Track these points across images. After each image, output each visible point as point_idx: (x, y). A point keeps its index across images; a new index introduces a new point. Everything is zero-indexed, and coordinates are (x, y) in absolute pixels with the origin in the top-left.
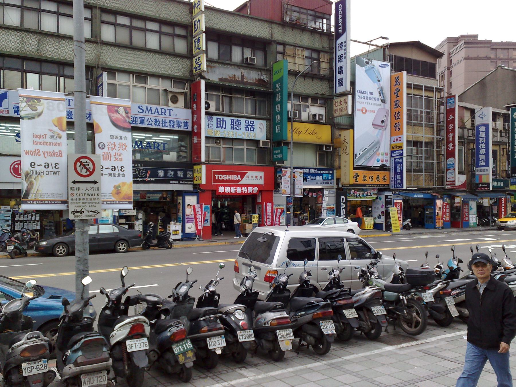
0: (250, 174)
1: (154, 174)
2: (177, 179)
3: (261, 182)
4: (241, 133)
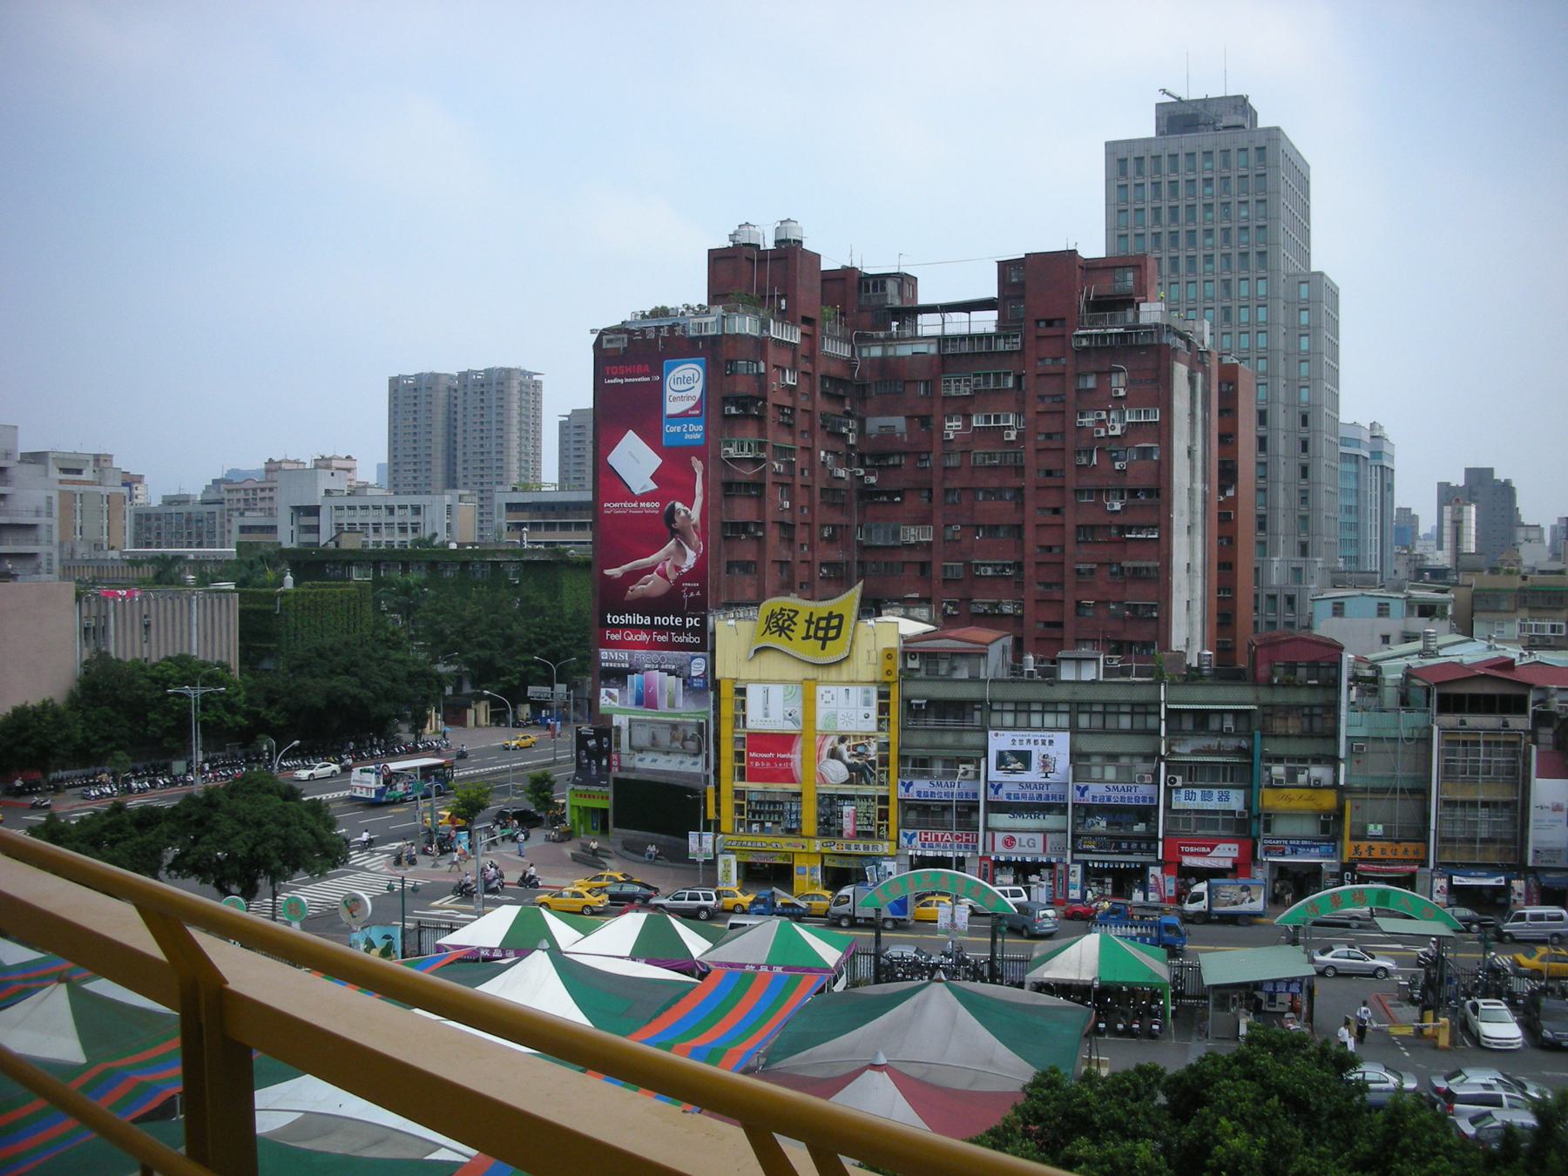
0: (1221, 846)
1: (1118, 846)
2: (1140, 850)
3: (1236, 854)
4: (1214, 804)
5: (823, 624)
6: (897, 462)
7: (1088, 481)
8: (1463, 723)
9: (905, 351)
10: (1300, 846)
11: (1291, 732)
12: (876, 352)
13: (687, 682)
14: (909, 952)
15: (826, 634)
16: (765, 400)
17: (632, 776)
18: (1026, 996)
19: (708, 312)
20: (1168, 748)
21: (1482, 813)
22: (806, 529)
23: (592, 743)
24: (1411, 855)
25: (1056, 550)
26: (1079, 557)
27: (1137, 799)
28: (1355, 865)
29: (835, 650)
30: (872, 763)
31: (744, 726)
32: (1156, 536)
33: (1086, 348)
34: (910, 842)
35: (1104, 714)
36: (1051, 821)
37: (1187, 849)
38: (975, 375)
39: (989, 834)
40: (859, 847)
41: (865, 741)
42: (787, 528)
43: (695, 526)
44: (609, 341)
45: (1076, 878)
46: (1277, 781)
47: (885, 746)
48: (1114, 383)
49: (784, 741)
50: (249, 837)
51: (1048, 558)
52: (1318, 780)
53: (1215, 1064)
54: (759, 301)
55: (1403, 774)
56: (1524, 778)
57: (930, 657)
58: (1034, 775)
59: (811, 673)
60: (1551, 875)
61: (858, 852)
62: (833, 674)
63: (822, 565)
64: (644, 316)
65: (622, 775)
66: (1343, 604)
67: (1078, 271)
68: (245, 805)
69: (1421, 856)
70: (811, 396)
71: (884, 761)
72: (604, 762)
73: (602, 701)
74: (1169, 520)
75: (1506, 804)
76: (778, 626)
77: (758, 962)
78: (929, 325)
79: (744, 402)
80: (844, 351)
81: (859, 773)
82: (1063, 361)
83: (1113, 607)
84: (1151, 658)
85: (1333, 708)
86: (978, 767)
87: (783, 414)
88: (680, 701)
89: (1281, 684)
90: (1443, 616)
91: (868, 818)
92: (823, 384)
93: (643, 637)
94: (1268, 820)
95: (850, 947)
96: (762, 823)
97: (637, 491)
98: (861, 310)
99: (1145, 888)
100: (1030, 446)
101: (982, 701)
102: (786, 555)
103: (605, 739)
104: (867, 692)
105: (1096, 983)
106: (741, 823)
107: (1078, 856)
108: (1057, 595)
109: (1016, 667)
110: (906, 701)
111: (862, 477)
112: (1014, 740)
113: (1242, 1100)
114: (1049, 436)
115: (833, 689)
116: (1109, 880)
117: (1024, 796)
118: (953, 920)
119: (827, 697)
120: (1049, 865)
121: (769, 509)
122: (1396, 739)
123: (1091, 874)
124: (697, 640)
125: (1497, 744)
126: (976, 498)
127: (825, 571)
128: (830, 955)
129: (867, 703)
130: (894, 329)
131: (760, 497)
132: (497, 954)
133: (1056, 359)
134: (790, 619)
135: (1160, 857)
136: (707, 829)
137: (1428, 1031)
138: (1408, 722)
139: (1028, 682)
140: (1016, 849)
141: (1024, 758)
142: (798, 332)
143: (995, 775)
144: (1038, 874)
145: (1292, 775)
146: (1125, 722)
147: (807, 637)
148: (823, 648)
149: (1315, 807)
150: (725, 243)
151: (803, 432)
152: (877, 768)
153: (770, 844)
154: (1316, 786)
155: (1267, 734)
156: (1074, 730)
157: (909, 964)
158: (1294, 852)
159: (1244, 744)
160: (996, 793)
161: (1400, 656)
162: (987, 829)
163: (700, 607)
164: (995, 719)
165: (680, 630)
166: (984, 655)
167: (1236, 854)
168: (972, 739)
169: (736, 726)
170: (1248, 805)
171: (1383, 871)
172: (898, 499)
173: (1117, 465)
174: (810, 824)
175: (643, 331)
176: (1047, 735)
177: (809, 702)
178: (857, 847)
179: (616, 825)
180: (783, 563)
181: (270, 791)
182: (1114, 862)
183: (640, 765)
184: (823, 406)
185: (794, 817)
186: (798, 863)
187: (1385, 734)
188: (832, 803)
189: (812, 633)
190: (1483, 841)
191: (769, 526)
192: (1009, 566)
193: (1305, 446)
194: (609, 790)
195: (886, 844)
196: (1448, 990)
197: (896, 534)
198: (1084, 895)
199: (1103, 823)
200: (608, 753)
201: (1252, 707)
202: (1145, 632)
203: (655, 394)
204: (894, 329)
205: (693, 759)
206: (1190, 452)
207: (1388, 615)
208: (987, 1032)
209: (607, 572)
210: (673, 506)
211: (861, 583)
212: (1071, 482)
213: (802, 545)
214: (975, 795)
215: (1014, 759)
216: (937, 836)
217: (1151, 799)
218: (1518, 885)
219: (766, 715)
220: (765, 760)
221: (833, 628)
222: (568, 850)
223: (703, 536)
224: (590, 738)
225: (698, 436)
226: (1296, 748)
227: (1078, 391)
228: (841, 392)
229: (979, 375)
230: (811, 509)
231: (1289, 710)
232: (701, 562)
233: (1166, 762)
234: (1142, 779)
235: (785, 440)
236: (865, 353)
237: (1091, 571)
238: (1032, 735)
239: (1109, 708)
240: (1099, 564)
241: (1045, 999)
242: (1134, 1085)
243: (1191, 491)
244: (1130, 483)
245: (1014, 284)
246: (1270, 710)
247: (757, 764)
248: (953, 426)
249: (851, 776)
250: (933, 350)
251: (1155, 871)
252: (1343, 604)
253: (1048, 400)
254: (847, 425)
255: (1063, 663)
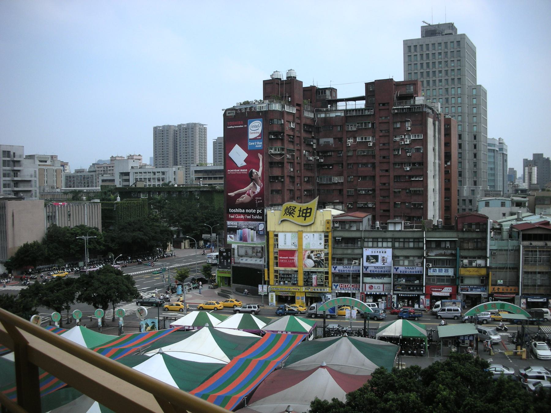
0: (446, 288)
1: (409, 288)
2: (417, 290)
3: (451, 291)
5: (305, 211)
6: (331, 154)
7: (398, 160)
8: (531, 244)
9: (333, 115)
10: (474, 288)
11: (470, 248)
12: (323, 115)
13: (258, 232)
14: (336, 326)
15: (306, 215)
16: (284, 133)
17: (239, 266)
18: (376, 342)
19: (263, 102)
20: (427, 254)
21: (538, 276)
22: (299, 178)
23: (225, 254)
24: (513, 291)
25: (387, 185)
26: (395, 187)
27: (416, 272)
28: (493, 294)
29: (309, 221)
30: (323, 260)
31: (278, 248)
32: (422, 179)
33: (396, 113)
34: (336, 288)
35: (404, 242)
36: (386, 280)
37: (434, 289)
38: (358, 123)
39: (364, 285)
40: (318, 290)
41: (320, 252)
42: (292, 178)
43: (260, 178)
44: (229, 113)
45: (395, 300)
46: (465, 265)
47: (327, 254)
48: (407, 125)
49: (291, 253)
50: (104, 288)
51: (384, 187)
52: (480, 265)
53: (438, 365)
54: (281, 98)
55: (510, 262)
57: (342, 223)
58: (379, 264)
59: (301, 229)
61: (318, 291)
62: (308, 229)
63: (305, 191)
64: (241, 104)
65: (235, 265)
66: (489, 202)
67: (394, 86)
68: (103, 277)
69: (517, 291)
70: (300, 132)
71: (327, 259)
72: (229, 261)
73: (228, 239)
74: (427, 174)
75: (547, 273)
76: (289, 212)
77: (282, 330)
78: (341, 106)
79: (276, 134)
80: (311, 115)
81: (318, 264)
82: (389, 118)
83: (407, 204)
84: (421, 222)
85: (485, 239)
86: (360, 261)
87: (290, 138)
88: (255, 239)
89: (466, 231)
90: (524, 206)
91: (321, 279)
92: (304, 127)
93: (242, 217)
94: (462, 279)
95: (315, 325)
96: (284, 282)
97: (239, 166)
98: (317, 101)
99: (419, 303)
100: (377, 148)
101: (361, 238)
102: (292, 187)
103: (229, 253)
104: (320, 235)
105: (401, 337)
106: (277, 281)
107: (395, 292)
108: (387, 200)
109: (373, 226)
110: (334, 238)
111: (318, 160)
112: (372, 252)
113: (447, 378)
114: (384, 144)
115: (308, 234)
116: (406, 301)
117: (376, 271)
118: (351, 315)
119: (307, 237)
120: (385, 295)
121: (286, 171)
122: (507, 250)
123: (400, 298)
124: (261, 218)
125: (543, 251)
126: (358, 166)
127: (306, 193)
128: (308, 327)
129: (321, 239)
130: (329, 107)
131: (283, 167)
132: (191, 328)
133: (386, 117)
134: (293, 210)
135: (424, 292)
136: (265, 284)
137: (519, 353)
138: (512, 244)
139: (377, 231)
140: (374, 290)
141: (376, 258)
142: (295, 110)
143: (366, 264)
144: (381, 298)
145: (470, 263)
146: (411, 245)
147: (299, 216)
148: (305, 220)
149: (479, 274)
150: (269, 78)
151: (297, 144)
152: (324, 262)
153: (286, 289)
154: (479, 267)
155: (462, 249)
156: (393, 248)
157: (336, 330)
158: (472, 290)
159: (453, 252)
160: (366, 270)
161: (509, 221)
162: (363, 283)
163: (262, 206)
164: (366, 244)
165: (255, 214)
166: (362, 222)
167: (451, 291)
168: (357, 251)
169: (275, 247)
170: (455, 274)
171: (503, 297)
172: (331, 167)
173: (408, 154)
174: (301, 282)
175: (240, 109)
176: (384, 250)
177: (300, 239)
178: (317, 290)
179: (233, 283)
180: (291, 190)
181: (112, 272)
182: (408, 294)
183: (241, 262)
184: (304, 135)
185: (295, 279)
186: (297, 295)
187: (503, 248)
188: (309, 274)
189: (301, 215)
190: (539, 286)
191: (286, 177)
192: (370, 190)
193: (475, 147)
194: (231, 270)
195: (328, 288)
196: (526, 338)
197: (331, 179)
198: (397, 306)
199: (404, 281)
200: (230, 258)
201: (456, 239)
202: (418, 213)
203: (245, 132)
204: (329, 107)
205: (260, 260)
206: (434, 150)
207: (505, 206)
208: (362, 354)
209: (229, 194)
210: (252, 171)
211: (318, 197)
212: (392, 160)
213: (297, 184)
214: (359, 271)
215: (372, 258)
216: (345, 286)
217: (421, 272)
219: (285, 244)
220: (285, 259)
221: (308, 213)
222: (216, 291)
223: (263, 181)
224: (224, 252)
225: (260, 146)
226: (472, 253)
227: (394, 128)
228: (310, 130)
229: (359, 123)
230: (300, 170)
231: (469, 240)
232: (262, 190)
233: (426, 259)
234: (417, 265)
235: (291, 147)
236: (319, 116)
237: (399, 192)
238: (379, 250)
239: (406, 240)
240: (402, 189)
241: (383, 343)
242: (410, 373)
243: (434, 163)
244: (413, 160)
245: (371, 91)
246: (463, 240)
247: (282, 261)
248: (350, 141)
249: (315, 265)
250: (343, 114)
251: (422, 297)
252: (489, 202)
253: (383, 132)
254: (313, 141)
255: (389, 224)
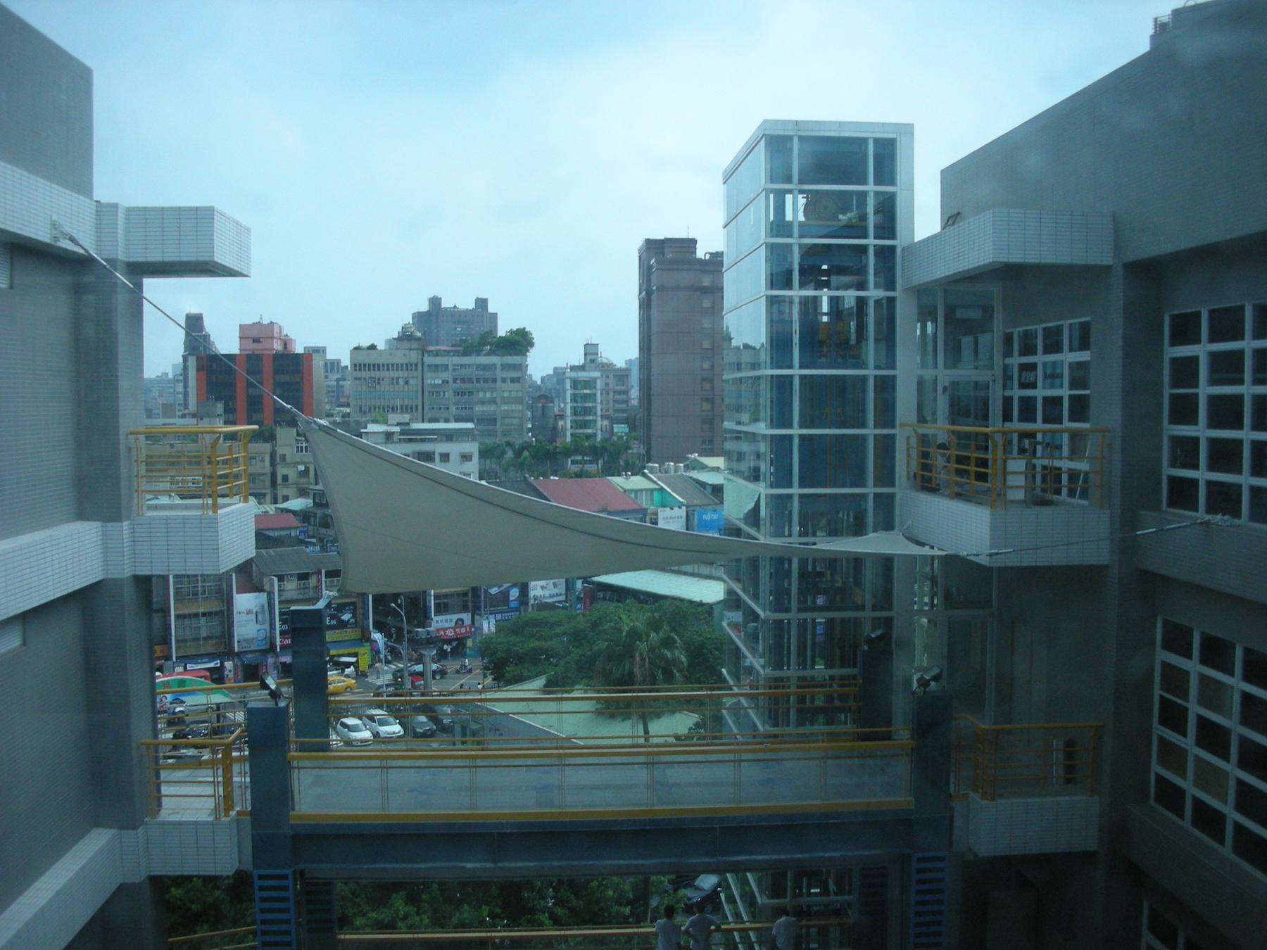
21: (203, 620)
56: (227, 594)
60: (250, 656)
75: (217, 613)
190: (206, 639)
218: (229, 665)
